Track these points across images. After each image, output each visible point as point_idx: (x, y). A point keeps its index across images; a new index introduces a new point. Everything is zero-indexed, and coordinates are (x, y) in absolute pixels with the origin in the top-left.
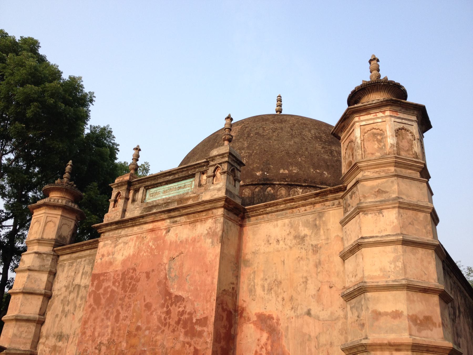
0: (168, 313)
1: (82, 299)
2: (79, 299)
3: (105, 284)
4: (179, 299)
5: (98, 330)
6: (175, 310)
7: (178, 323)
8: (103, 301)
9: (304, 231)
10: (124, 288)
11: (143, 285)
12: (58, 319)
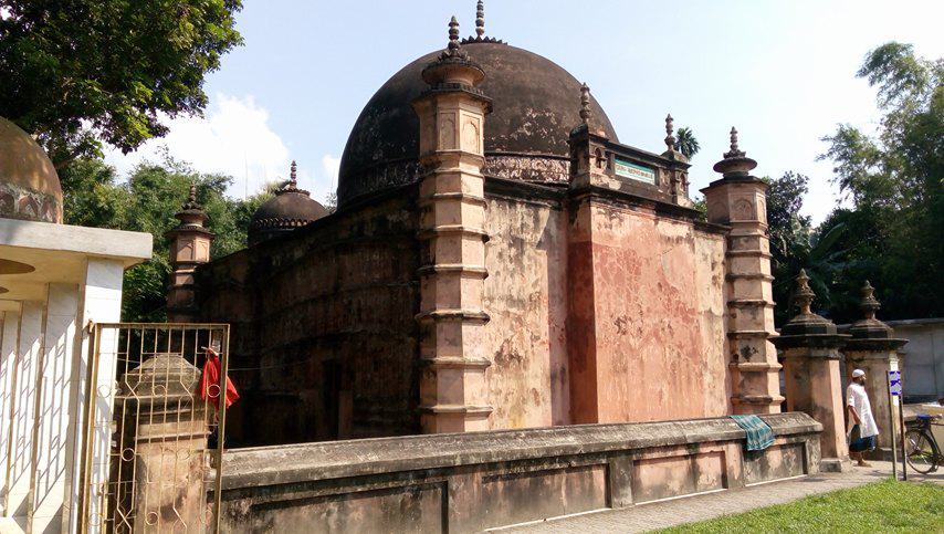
0: (669, 300)
1: (530, 259)
2: (525, 257)
3: (610, 260)
4: (674, 290)
5: (613, 306)
6: (674, 299)
7: (677, 309)
8: (612, 277)
9: (708, 252)
10: (629, 268)
11: (643, 269)
12: (500, 279)
